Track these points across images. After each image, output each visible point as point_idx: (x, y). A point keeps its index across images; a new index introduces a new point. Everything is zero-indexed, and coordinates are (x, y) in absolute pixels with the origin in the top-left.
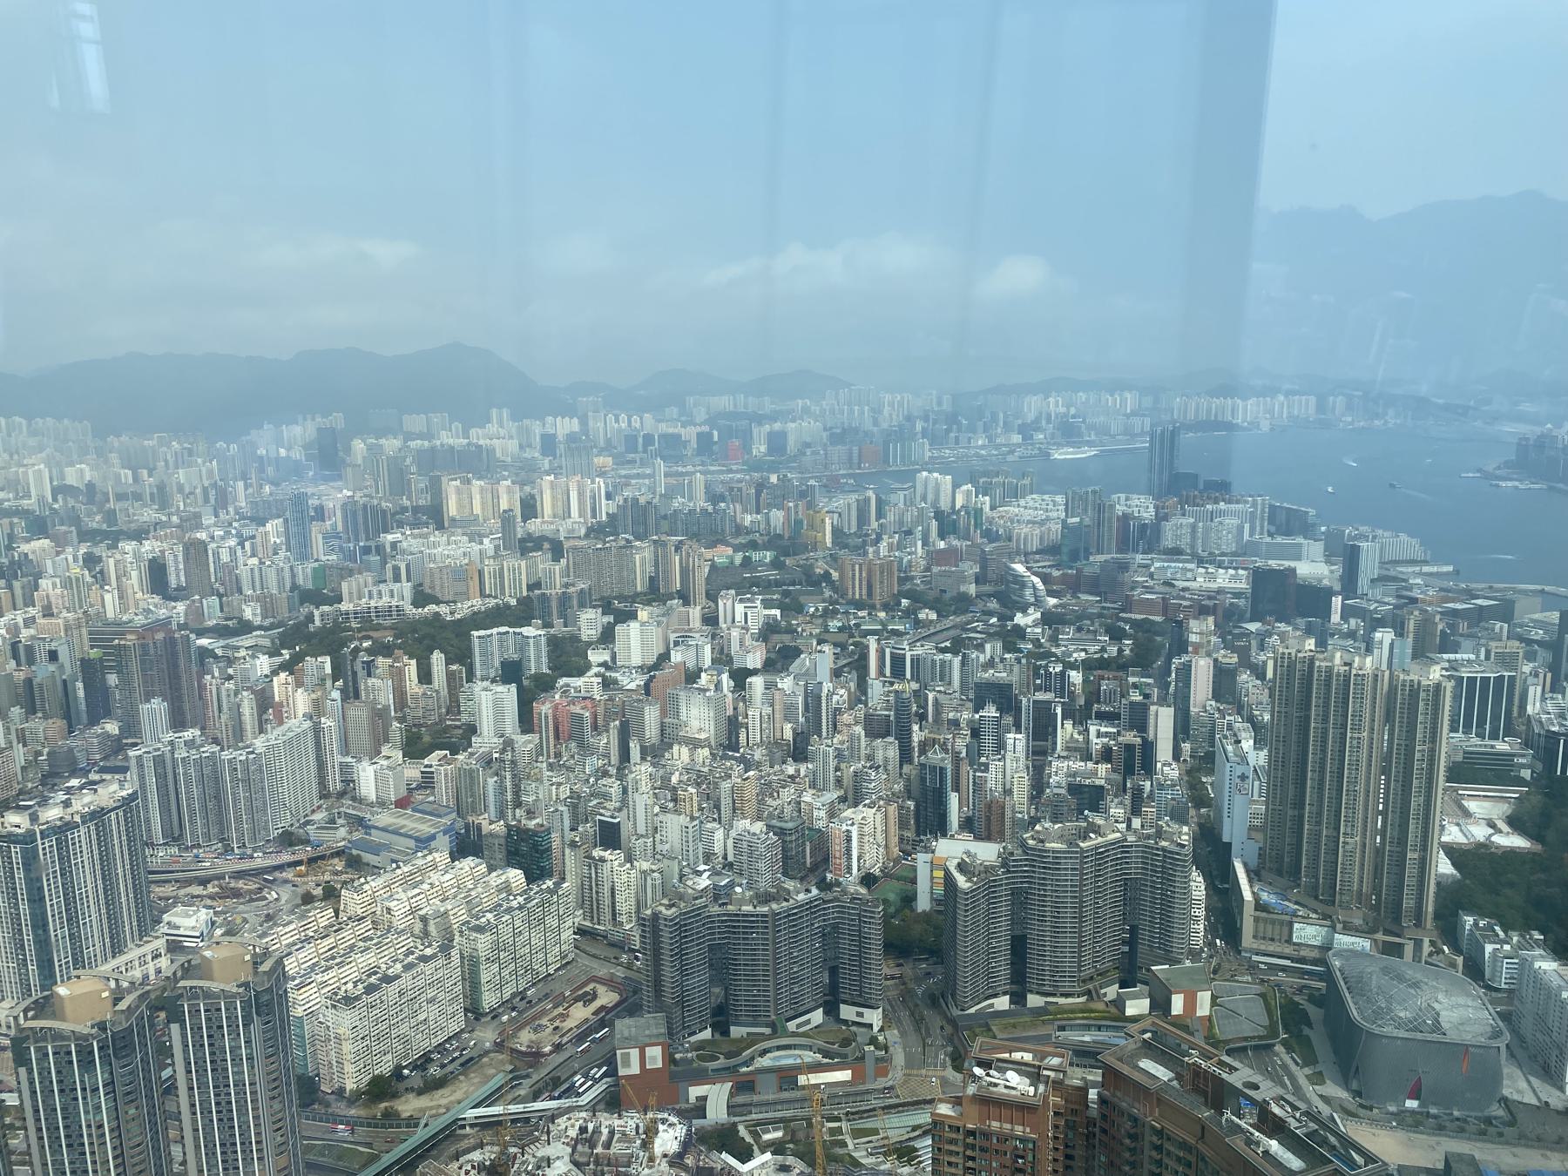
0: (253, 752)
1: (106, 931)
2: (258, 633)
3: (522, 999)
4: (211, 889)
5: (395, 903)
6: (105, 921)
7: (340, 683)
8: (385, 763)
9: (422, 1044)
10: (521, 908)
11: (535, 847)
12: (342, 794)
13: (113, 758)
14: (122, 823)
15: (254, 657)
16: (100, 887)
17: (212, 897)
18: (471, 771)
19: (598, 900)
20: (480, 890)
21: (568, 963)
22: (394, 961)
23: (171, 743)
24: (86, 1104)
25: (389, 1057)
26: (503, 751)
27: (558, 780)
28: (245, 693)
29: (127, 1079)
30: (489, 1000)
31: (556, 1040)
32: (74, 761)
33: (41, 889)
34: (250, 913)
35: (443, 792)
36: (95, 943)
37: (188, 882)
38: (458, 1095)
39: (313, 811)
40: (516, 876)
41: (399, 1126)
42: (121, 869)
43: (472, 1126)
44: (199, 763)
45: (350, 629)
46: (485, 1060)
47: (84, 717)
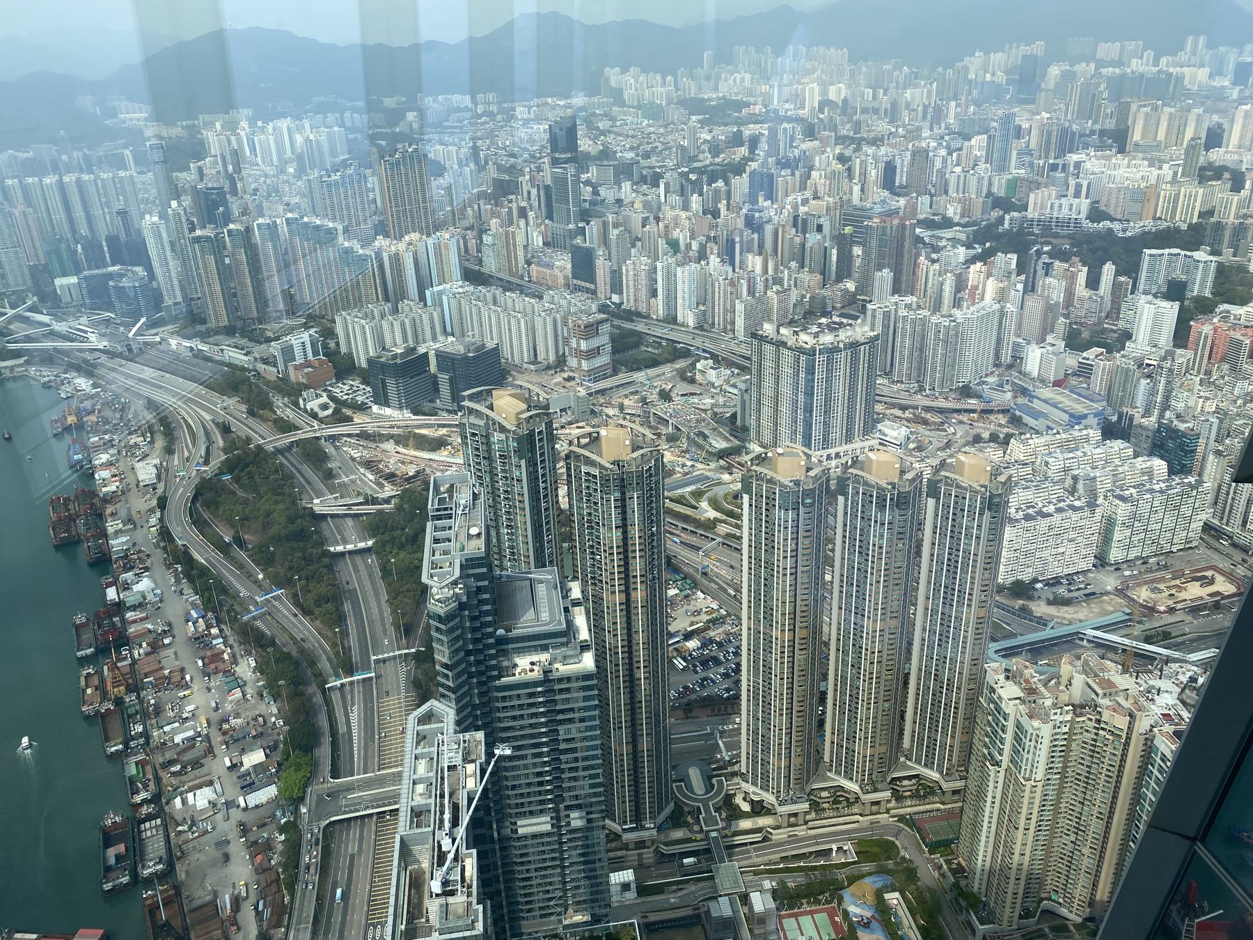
0: (954, 321)
1: (845, 425)
2: (957, 228)
3: (1144, 563)
4: (907, 414)
5: (1053, 459)
6: (845, 418)
7: (1023, 277)
8: (1050, 348)
9: (1055, 569)
10: (1161, 492)
11: (1181, 446)
12: (1010, 367)
13: (855, 306)
14: (867, 354)
15: (954, 247)
16: (847, 395)
17: (908, 420)
18: (1128, 370)
19: (1232, 505)
20: (1126, 468)
21: (1190, 548)
22: (1050, 503)
23: (896, 304)
24: (875, 531)
25: (1030, 570)
26: (1164, 359)
27: (1207, 394)
28: (949, 275)
29: (902, 524)
30: (1115, 554)
31: (1170, 603)
32: (825, 306)
33: (813, 387)
34: (935, 439)
35: (1098, 382)
36: (837, 432)
37: (893, 406)
38: (1081, 616)
39: (987, 375)
40: (1159, 465)
41: (1031, 620)
42: (860, 387)
43: (1089, 641)
44: (914, 322)
45: (1033, 234)
46: (1105, 598)
47: (833, 274)
